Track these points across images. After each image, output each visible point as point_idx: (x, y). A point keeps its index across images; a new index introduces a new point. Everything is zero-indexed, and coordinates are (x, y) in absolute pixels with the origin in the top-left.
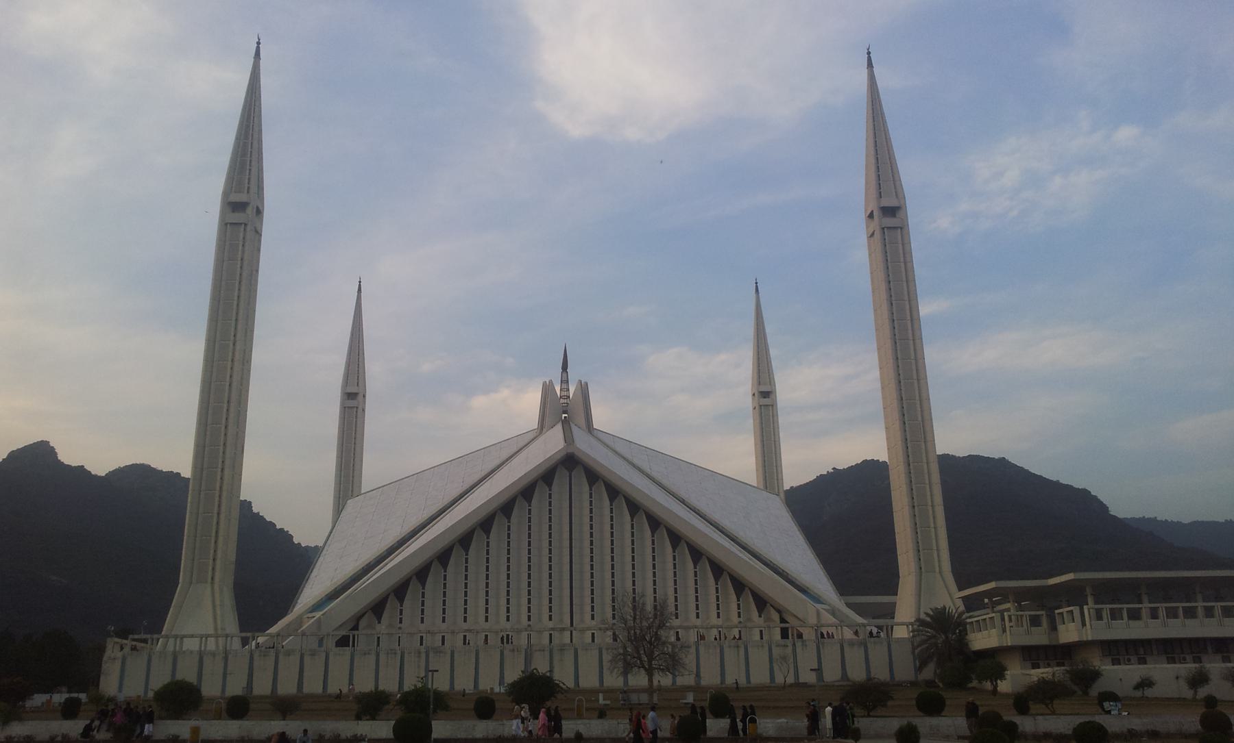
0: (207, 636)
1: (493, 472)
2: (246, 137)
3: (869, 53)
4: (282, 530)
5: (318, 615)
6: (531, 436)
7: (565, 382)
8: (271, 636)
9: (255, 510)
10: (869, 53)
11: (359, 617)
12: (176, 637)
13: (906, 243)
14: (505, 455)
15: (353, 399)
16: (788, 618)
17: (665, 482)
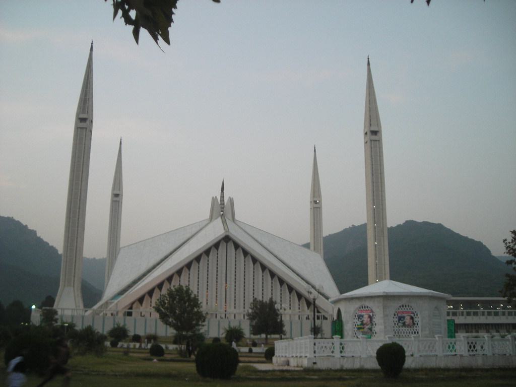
0: (74, 309)
1: (188, 240)
2: (87, 88)
3: (368, 59)
4: (52, 247)
5: (116, 301)
6: (206, 222)
7: (222, 197)
8: (94, 310)
9: (38, 235)
10: (368, 59)
11: (133, 303)
12: (62, 309)
13: (381, 148)
14: (194, 230)
15: (117, 196)
16: (320, 311)
17: (269, 248)
